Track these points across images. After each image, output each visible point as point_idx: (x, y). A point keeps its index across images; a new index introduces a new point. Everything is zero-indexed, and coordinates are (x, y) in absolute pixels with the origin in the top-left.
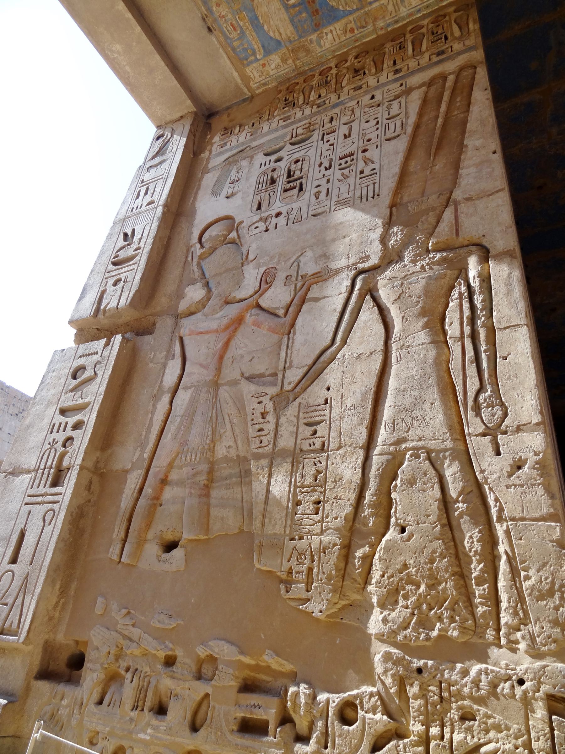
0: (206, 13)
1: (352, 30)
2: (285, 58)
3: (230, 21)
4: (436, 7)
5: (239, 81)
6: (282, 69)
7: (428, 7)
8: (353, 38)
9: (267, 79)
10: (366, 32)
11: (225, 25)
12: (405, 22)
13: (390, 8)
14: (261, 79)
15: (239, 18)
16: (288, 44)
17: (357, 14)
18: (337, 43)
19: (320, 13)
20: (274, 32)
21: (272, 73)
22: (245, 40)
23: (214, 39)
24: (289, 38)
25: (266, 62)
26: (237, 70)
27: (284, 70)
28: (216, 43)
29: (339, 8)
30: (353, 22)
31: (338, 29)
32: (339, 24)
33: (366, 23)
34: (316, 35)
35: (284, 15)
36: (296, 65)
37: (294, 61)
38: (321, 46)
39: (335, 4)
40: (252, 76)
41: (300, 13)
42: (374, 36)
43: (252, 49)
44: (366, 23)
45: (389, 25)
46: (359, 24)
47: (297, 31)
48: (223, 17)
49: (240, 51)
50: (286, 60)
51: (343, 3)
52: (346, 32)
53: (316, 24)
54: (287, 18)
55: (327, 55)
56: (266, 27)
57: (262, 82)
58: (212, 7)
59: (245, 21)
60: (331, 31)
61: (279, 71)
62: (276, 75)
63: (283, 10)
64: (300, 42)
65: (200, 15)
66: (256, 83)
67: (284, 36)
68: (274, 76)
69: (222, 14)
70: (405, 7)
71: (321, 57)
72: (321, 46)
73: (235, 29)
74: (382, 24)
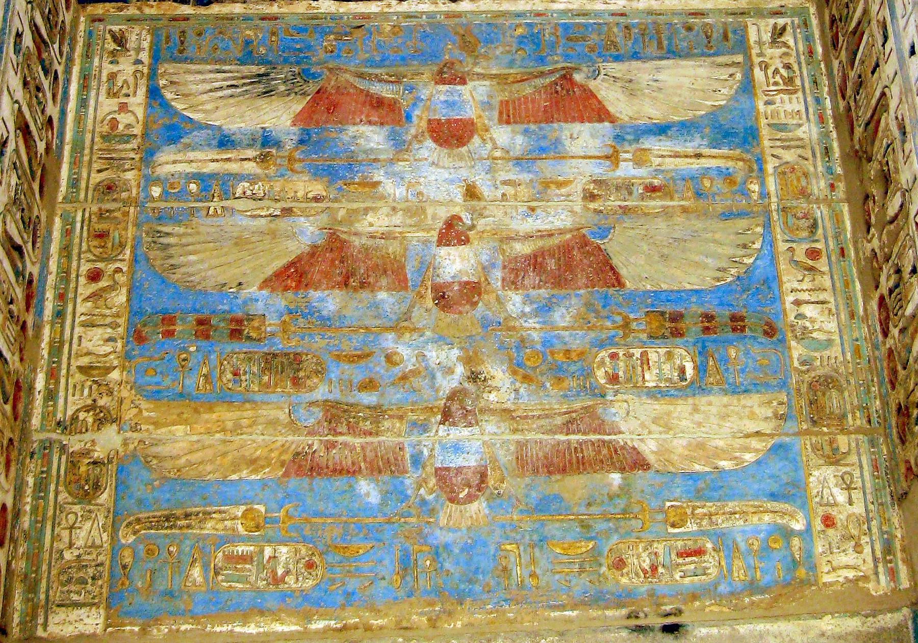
0: (624, 612)
1: (813, 254)
2: (827, 448)
3: (674, 556)
4: (822, 65)
5: (853, 624)
6: (857, 473)
7: (815, 82)
8: (833, 258)
9: (875, 530)
10: (828, 225)
11: (677, 576)
12: (834, 135)
13: (789, 156)
14: (867, 550)
15: (673, 525)
16: (792, 427)
17: (778, 230)
18: (832, 300)
19: (744, 312)
20: (747, 449)
21: (858, 509)
22: (739, 539)
23: (704, 631)
24: (777, 416)
25: (821, 511)
26: (817, 615)
27: (861, 467)
28: (715, 631)
29: (749, 266)
30: (794, 245)
31: (796, 285)
32: (785, 279)
33: (805, 216)
34: (793, 343)
35: (714, 403)
36: (859, 430)
37: (844, 431)
38: (830, 342)
39: (733, 271)
40: (851, 574)
41: (726, 360)
42: (845, 208)
43: (770, 534)
44: (805, 216)
45: (829, 170)
46: (805, 234)
47: (767, 385)
48: (654, 568)
49: (762, 571)
50: (835, 450)
51: (741, 252)
52: (811, 269)
53: (766, 333)
54: (725, 399)
55: (856, 335)
56: (726, 464)
57: (879, 554)
58: (618, 582)
59: (689, 511)
60: (797, 303)
61: (860, 484)
62: (869, 497)
63: (702, 400)
64: (799, 390)
65: (624, 634)
66: (876, 574)
67: (767, 428)
68: (871, 507)
69: (646, 565)
70: (800, 125)
71: (857, 352)
72: (830, 342)
73: (699, 552)
74: (822, 184)
